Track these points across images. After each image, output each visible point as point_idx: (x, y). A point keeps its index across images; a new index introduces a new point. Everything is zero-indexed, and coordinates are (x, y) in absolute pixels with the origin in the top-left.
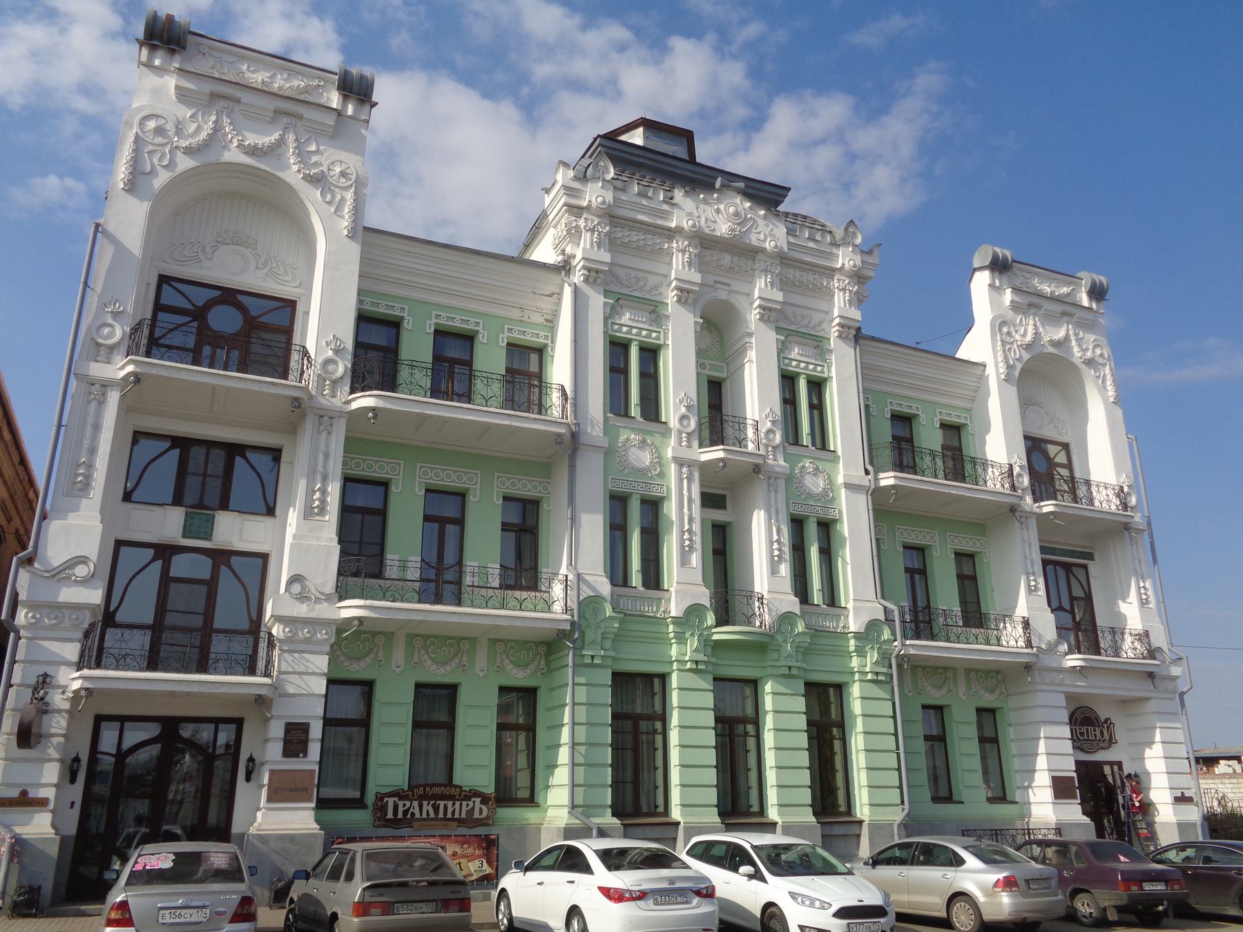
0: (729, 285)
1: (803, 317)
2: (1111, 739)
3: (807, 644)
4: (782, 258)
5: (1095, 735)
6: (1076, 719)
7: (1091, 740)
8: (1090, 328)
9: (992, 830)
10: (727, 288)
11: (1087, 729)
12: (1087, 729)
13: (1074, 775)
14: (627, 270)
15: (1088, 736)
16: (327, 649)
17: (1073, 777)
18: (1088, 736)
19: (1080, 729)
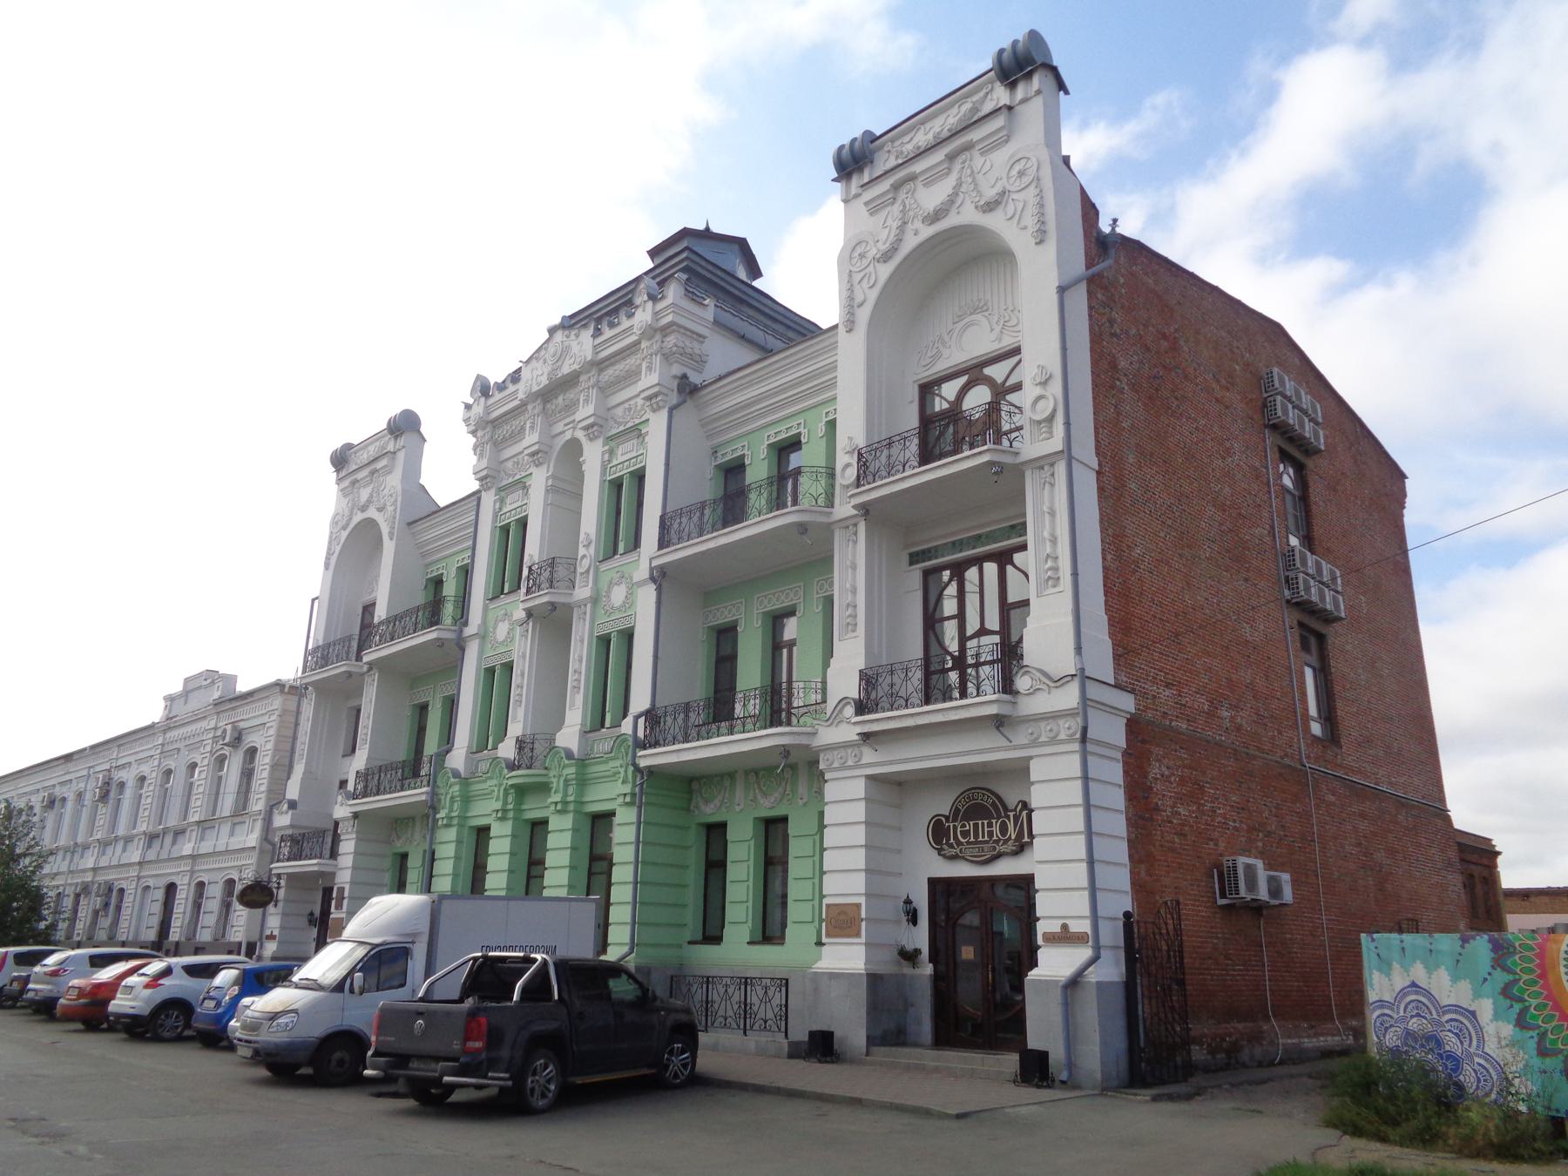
0: (574, 421)
1: (630, 409)
2: (1020, 835)
3: (574, 776)
4: (599, 365)
5: (991, 834)
6: (957, 811)
7: (981, 842)
8: (1007, 141)
9: (781, 979)
10: (571, 425)
11: (976, 826)
12: (976, 826)
13: (862, 900)
14: (512, 460)
15: (976, 836)
16: (354, 836)
17: (858, 906)
18: (976, 836)
19: (964, 826)
